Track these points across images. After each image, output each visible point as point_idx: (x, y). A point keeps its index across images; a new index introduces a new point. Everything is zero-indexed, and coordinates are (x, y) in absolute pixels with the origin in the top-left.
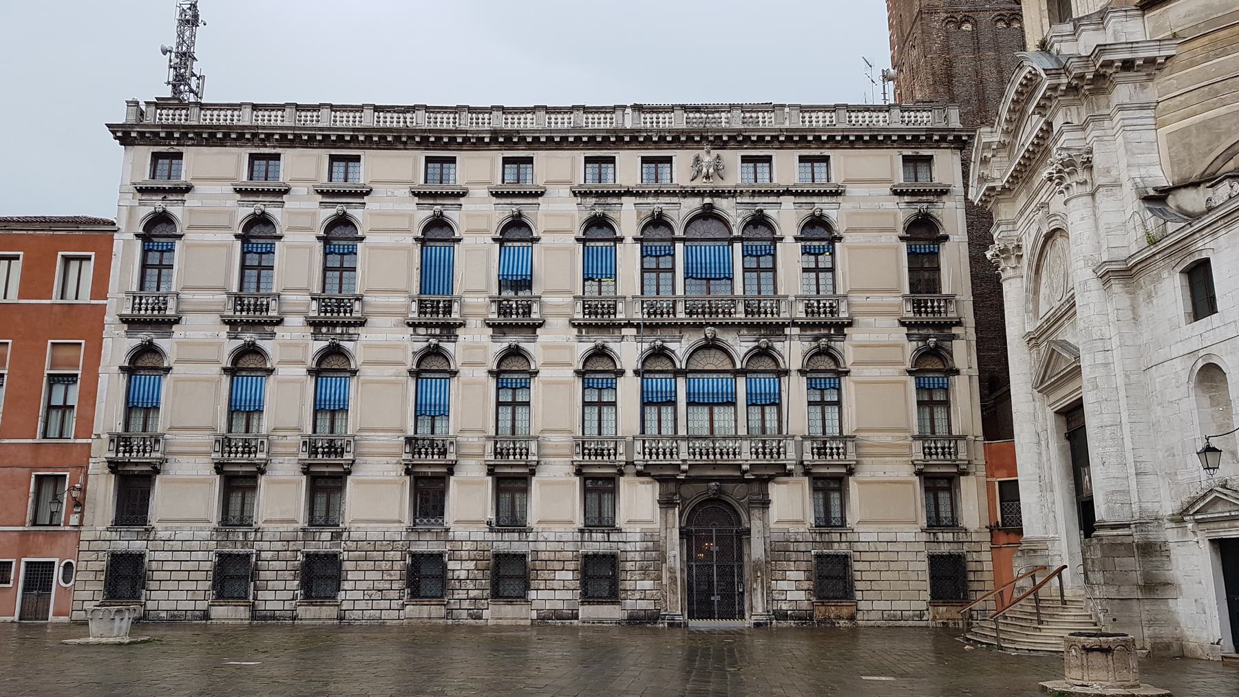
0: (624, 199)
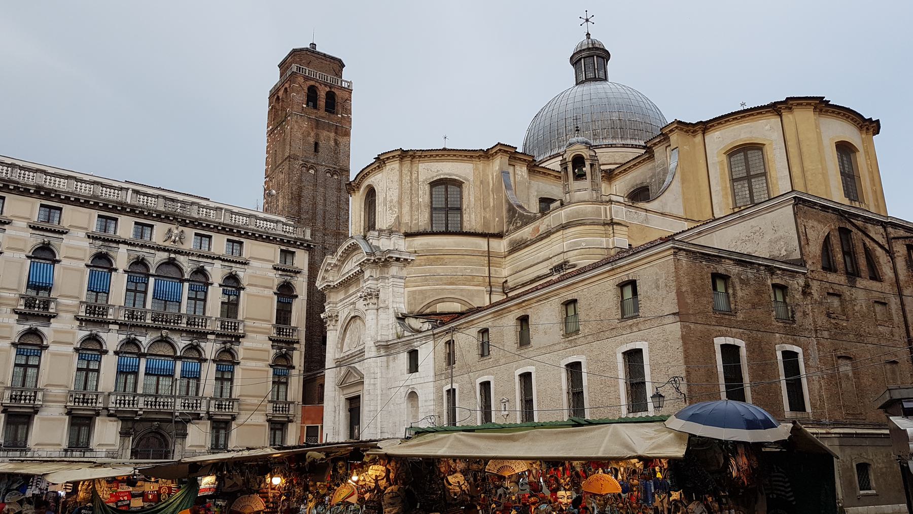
0: (121, 246)
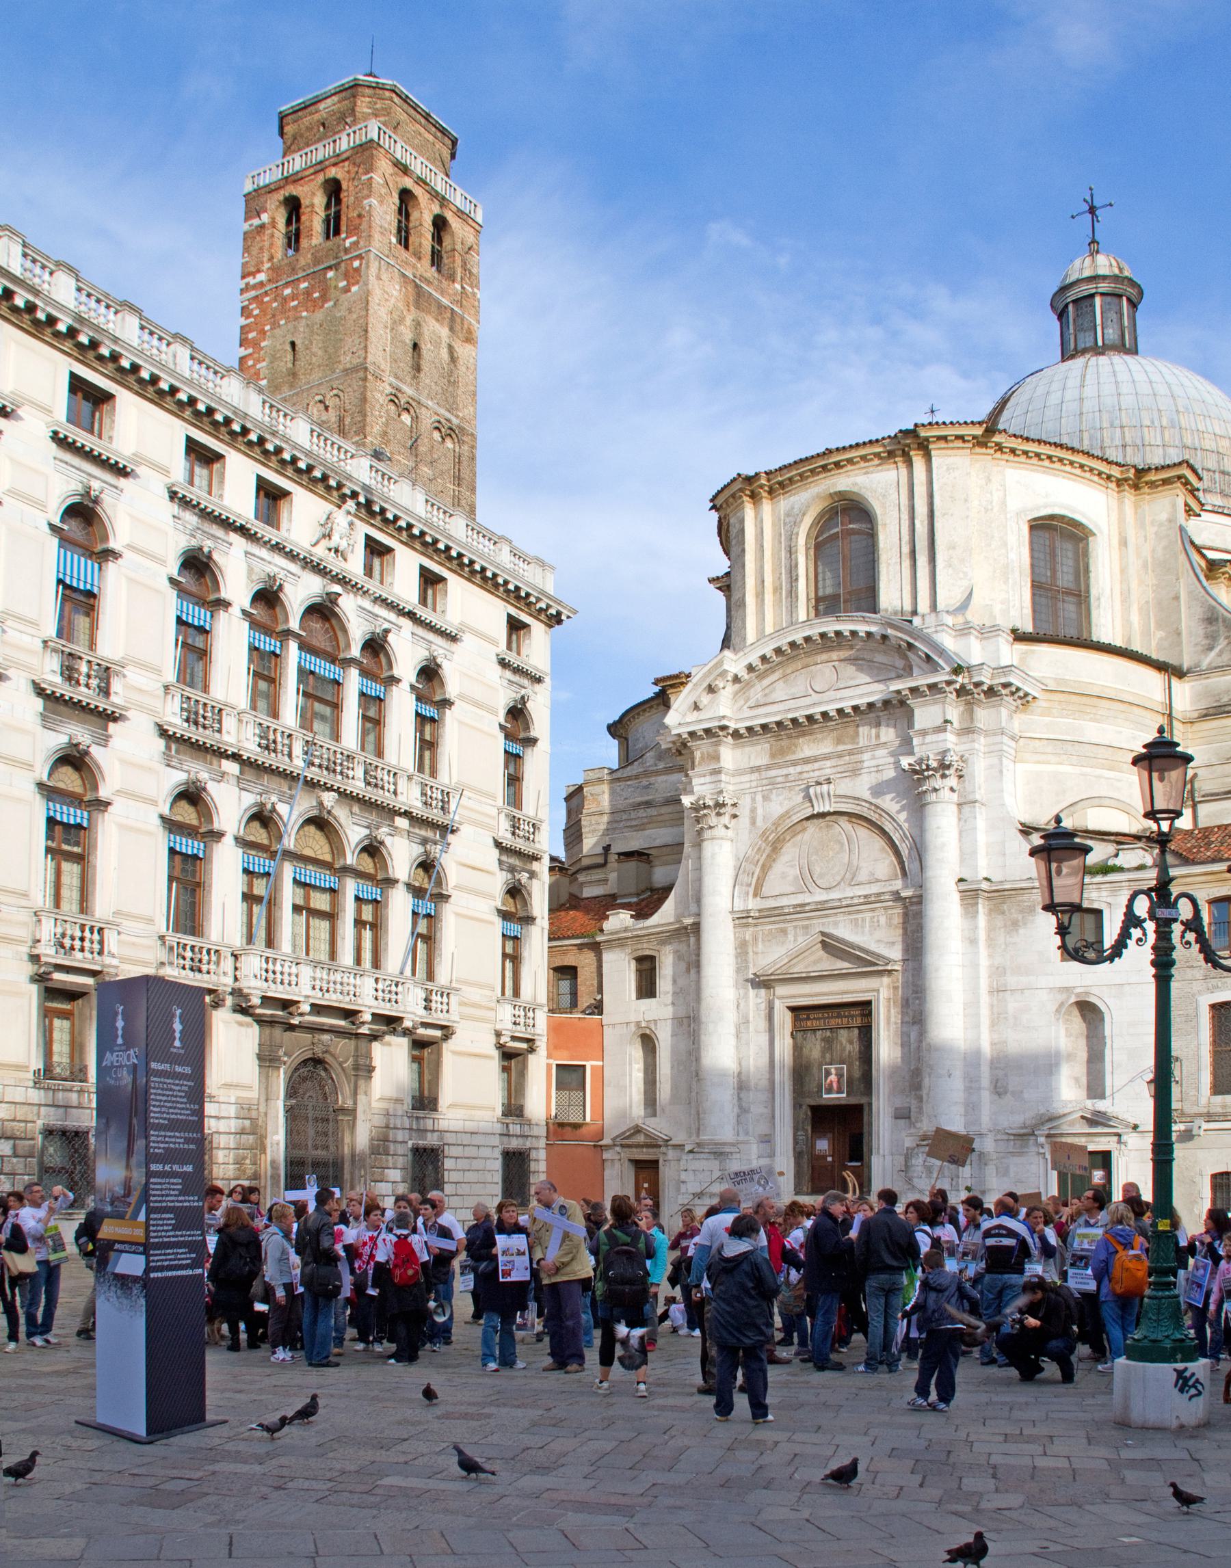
0: (234, 537)
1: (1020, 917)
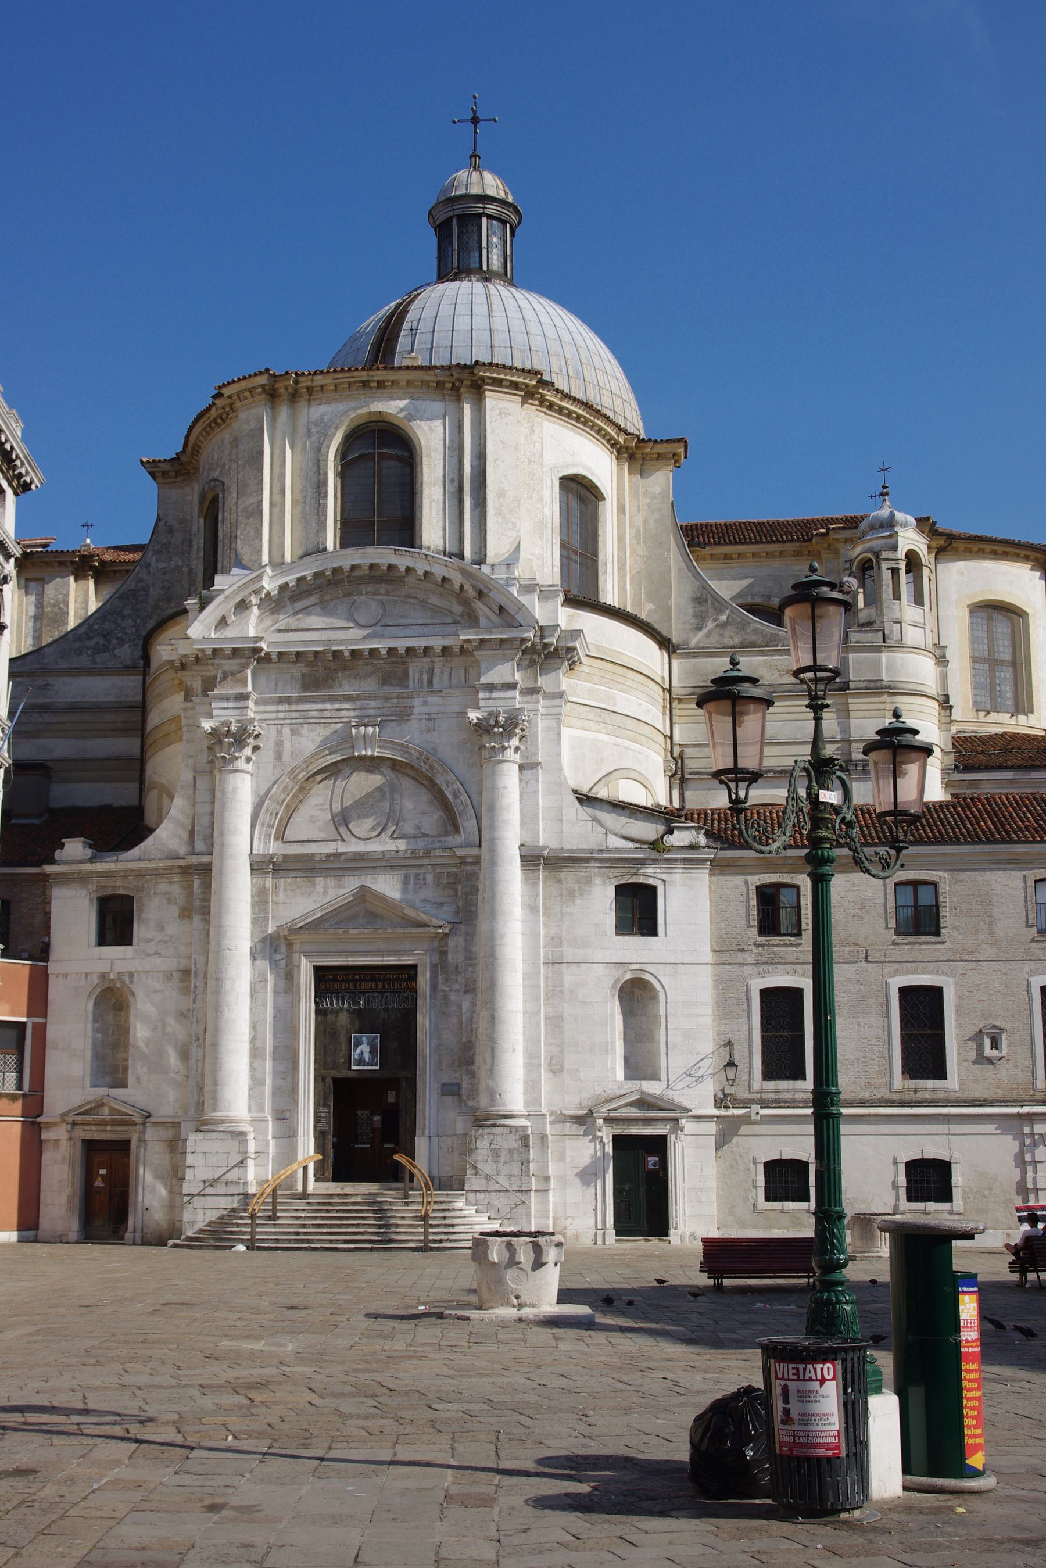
1: (577, 887)
